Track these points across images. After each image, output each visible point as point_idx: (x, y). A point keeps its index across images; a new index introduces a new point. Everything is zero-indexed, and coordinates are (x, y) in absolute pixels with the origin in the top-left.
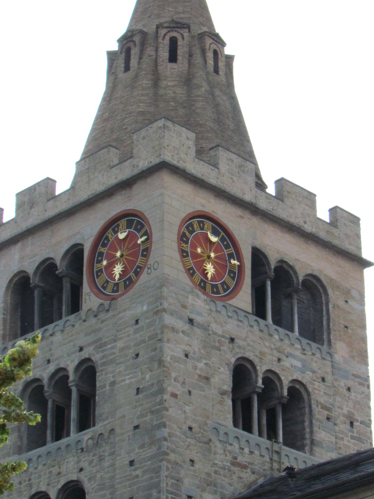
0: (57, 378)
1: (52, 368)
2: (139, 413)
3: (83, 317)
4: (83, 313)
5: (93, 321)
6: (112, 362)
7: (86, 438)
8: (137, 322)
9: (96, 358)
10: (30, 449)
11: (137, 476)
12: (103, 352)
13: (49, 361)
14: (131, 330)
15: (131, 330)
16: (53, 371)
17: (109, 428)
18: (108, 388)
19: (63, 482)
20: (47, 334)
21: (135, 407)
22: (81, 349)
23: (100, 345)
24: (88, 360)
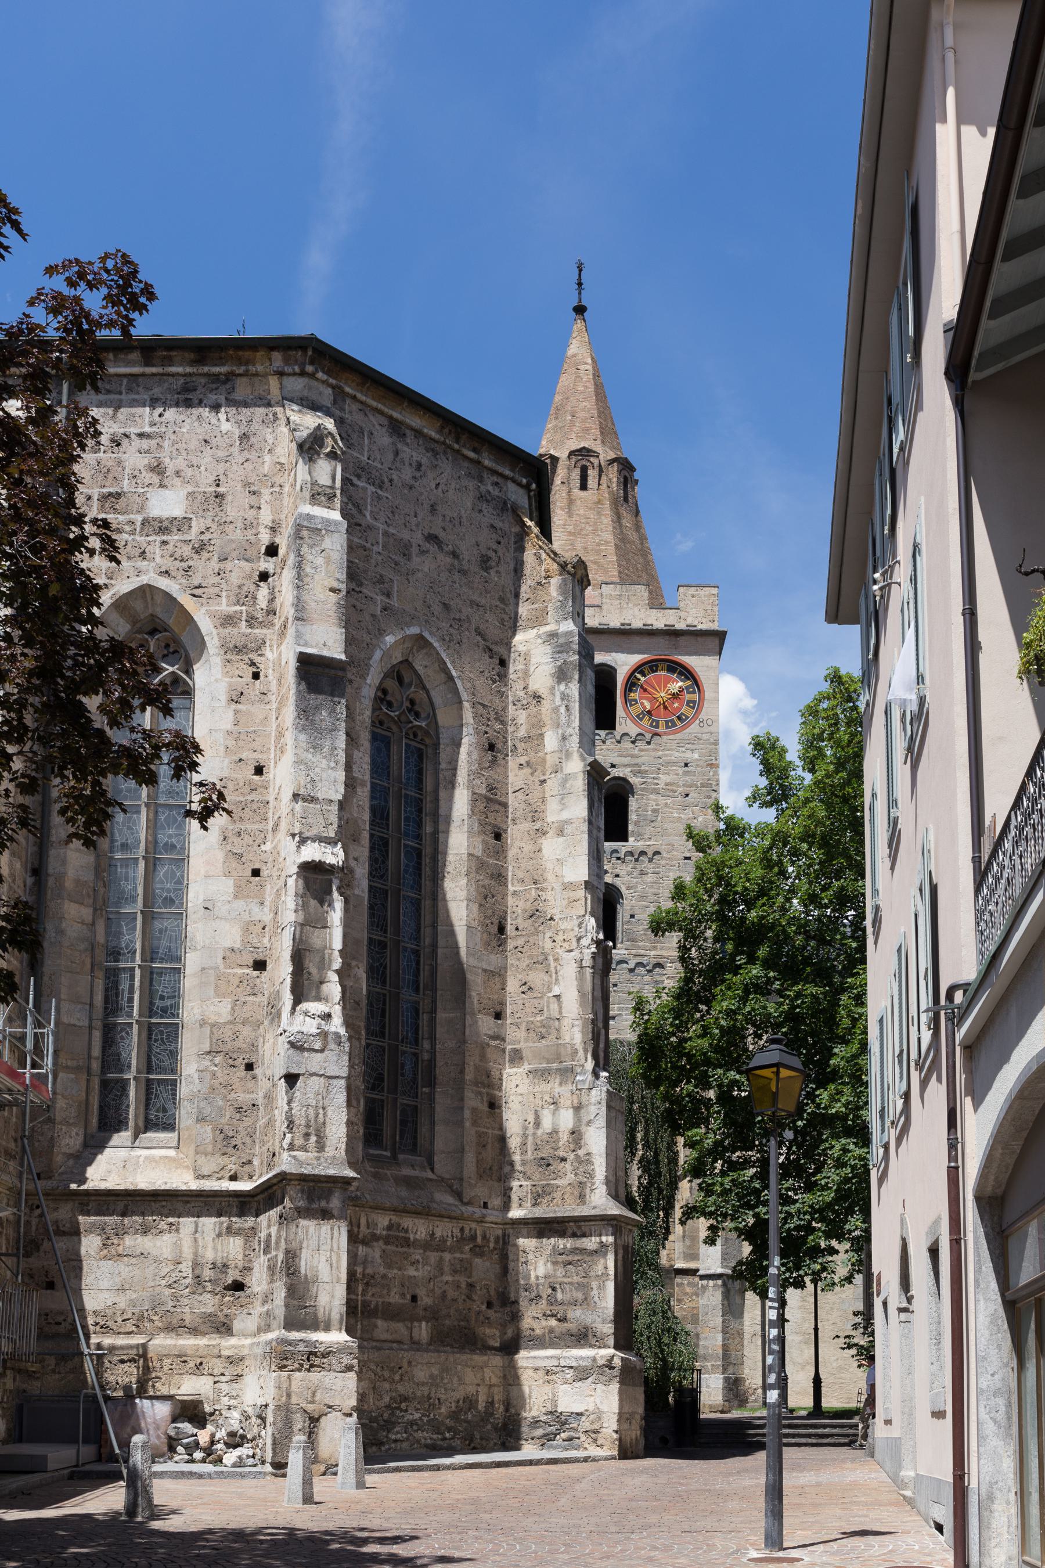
5: (627, 744)
8: (686, 765)
9: (634, 780)
12: (643, 778)
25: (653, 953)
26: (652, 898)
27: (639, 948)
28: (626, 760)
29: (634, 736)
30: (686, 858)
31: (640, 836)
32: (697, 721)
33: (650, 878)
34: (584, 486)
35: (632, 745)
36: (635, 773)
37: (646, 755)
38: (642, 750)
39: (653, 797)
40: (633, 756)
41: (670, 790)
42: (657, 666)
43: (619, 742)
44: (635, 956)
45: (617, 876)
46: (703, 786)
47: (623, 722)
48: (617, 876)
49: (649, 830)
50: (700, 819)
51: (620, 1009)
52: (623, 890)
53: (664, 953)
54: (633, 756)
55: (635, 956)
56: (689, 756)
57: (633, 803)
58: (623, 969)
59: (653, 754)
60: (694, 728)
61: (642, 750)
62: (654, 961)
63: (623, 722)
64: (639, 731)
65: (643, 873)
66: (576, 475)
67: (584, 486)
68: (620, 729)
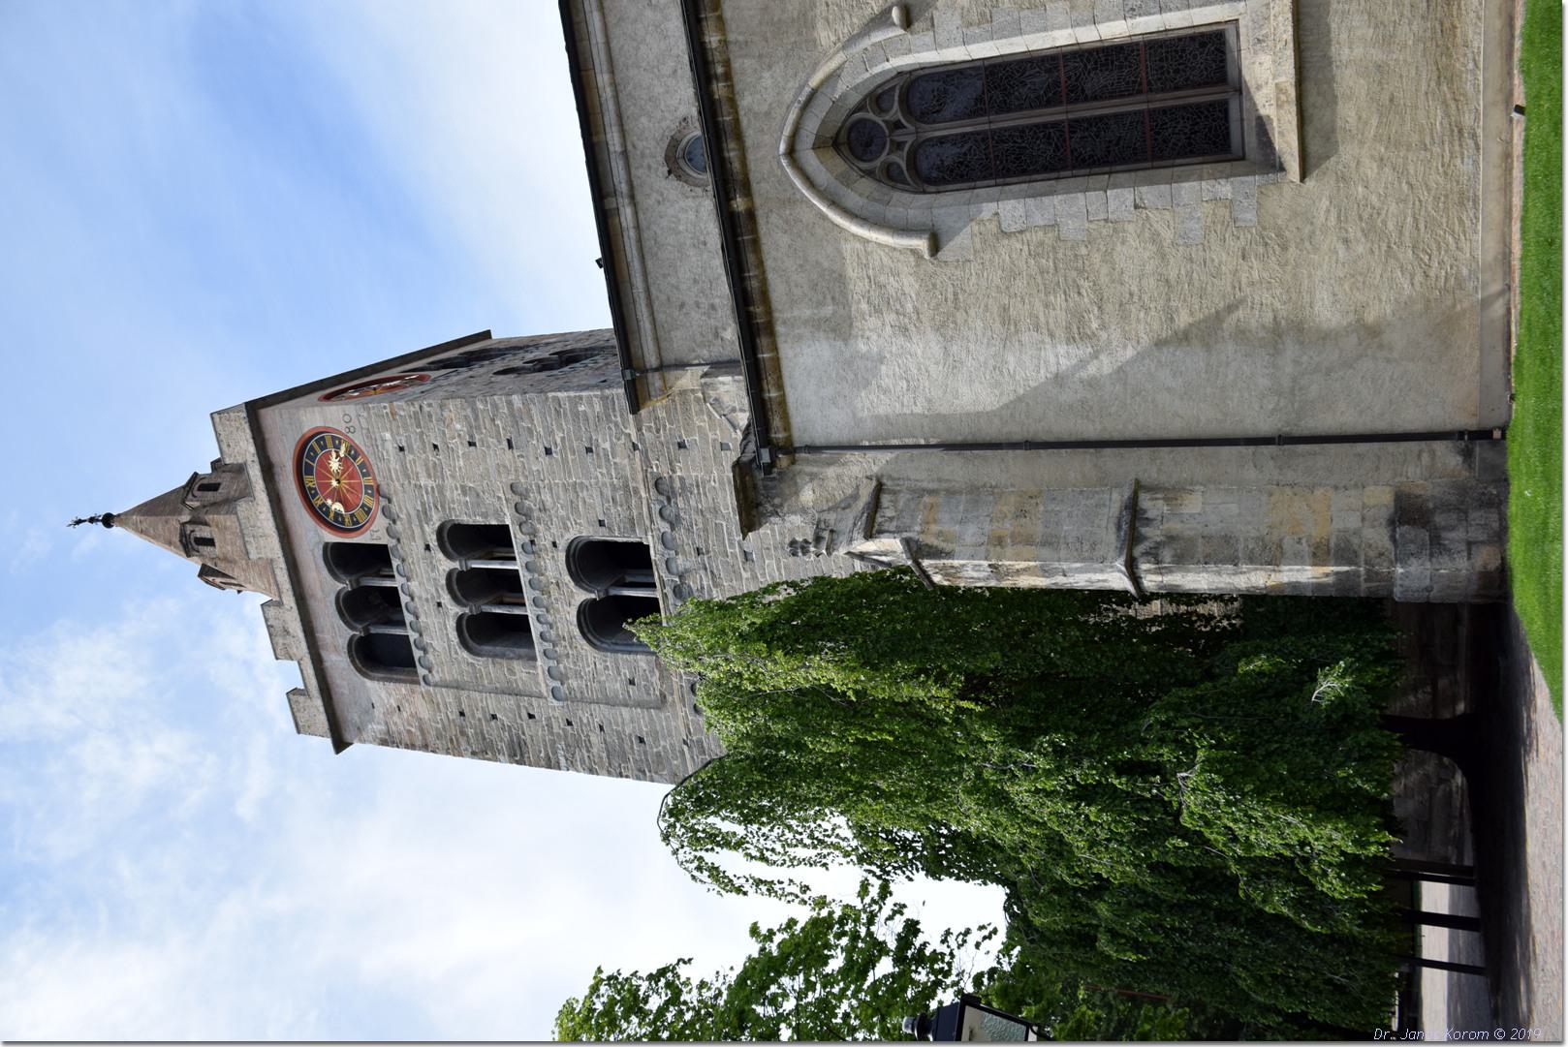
0: (459, 594)
1: (446, 598)
2: (495, 441)
3: (394, 541)
4: (391, 543)
5: (399, 526)
6: (441, 489)
7: (520, 535)
8: (402, 449)
9: (436, 520)
10: (530, 644)
11: (563, 439)
13: (439, 605)
14: (410, 457)
15: (410, 457)
16: (449, 597)
17: (510, 495)
18: (468, 499)
19: (567, 578)
20: (412, 605)
21: (489, 447)
22: (428, 547)
23: (424, 515)
24: (440, 532)
25: (643, 495)
26: (572, 495)
27: (641, 514)
28: (417, 531)
29: (387, 521)
30: (510, 446)
31: (498, 513)
32: (350, 435)
33: (547, 497)
34: (210, 542)
35: (398, 523)
36: (428, 520)
37: (405, 504)
38: (400, 508)
39: (448, 494)
40: (410, 522)
41: (434, 471)
42: (310, 489)
43: (399, 540)
44: (652, 521)
45: (554, 544)
46: (419, 426)
47: (376, 535)
48: (554, 544)
49: (488, 499)
50: (458, 426)
51: (732, 545)
52: (570, 536)
53: (640, 476)
54: (410, 522)
55: (652, 521)
56: (391, 447)
57: (466, 520)
58: (674, 539)
59: (401, 495)
60: (359, 440)
61: (400, 508)
62: (653, 491)
63: (376, 535)
64: (380, 512)
65: (543, 509)
66: (206, 550)
67: (210, 542)
68: (384, 540)
